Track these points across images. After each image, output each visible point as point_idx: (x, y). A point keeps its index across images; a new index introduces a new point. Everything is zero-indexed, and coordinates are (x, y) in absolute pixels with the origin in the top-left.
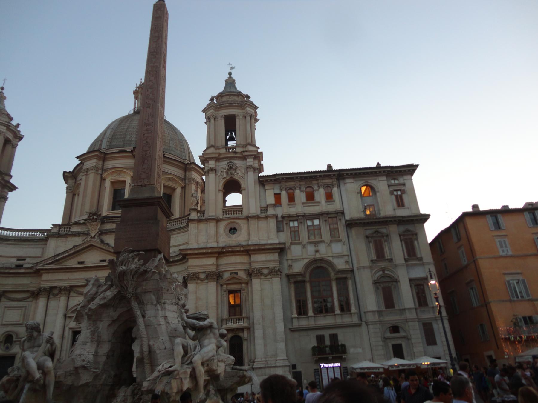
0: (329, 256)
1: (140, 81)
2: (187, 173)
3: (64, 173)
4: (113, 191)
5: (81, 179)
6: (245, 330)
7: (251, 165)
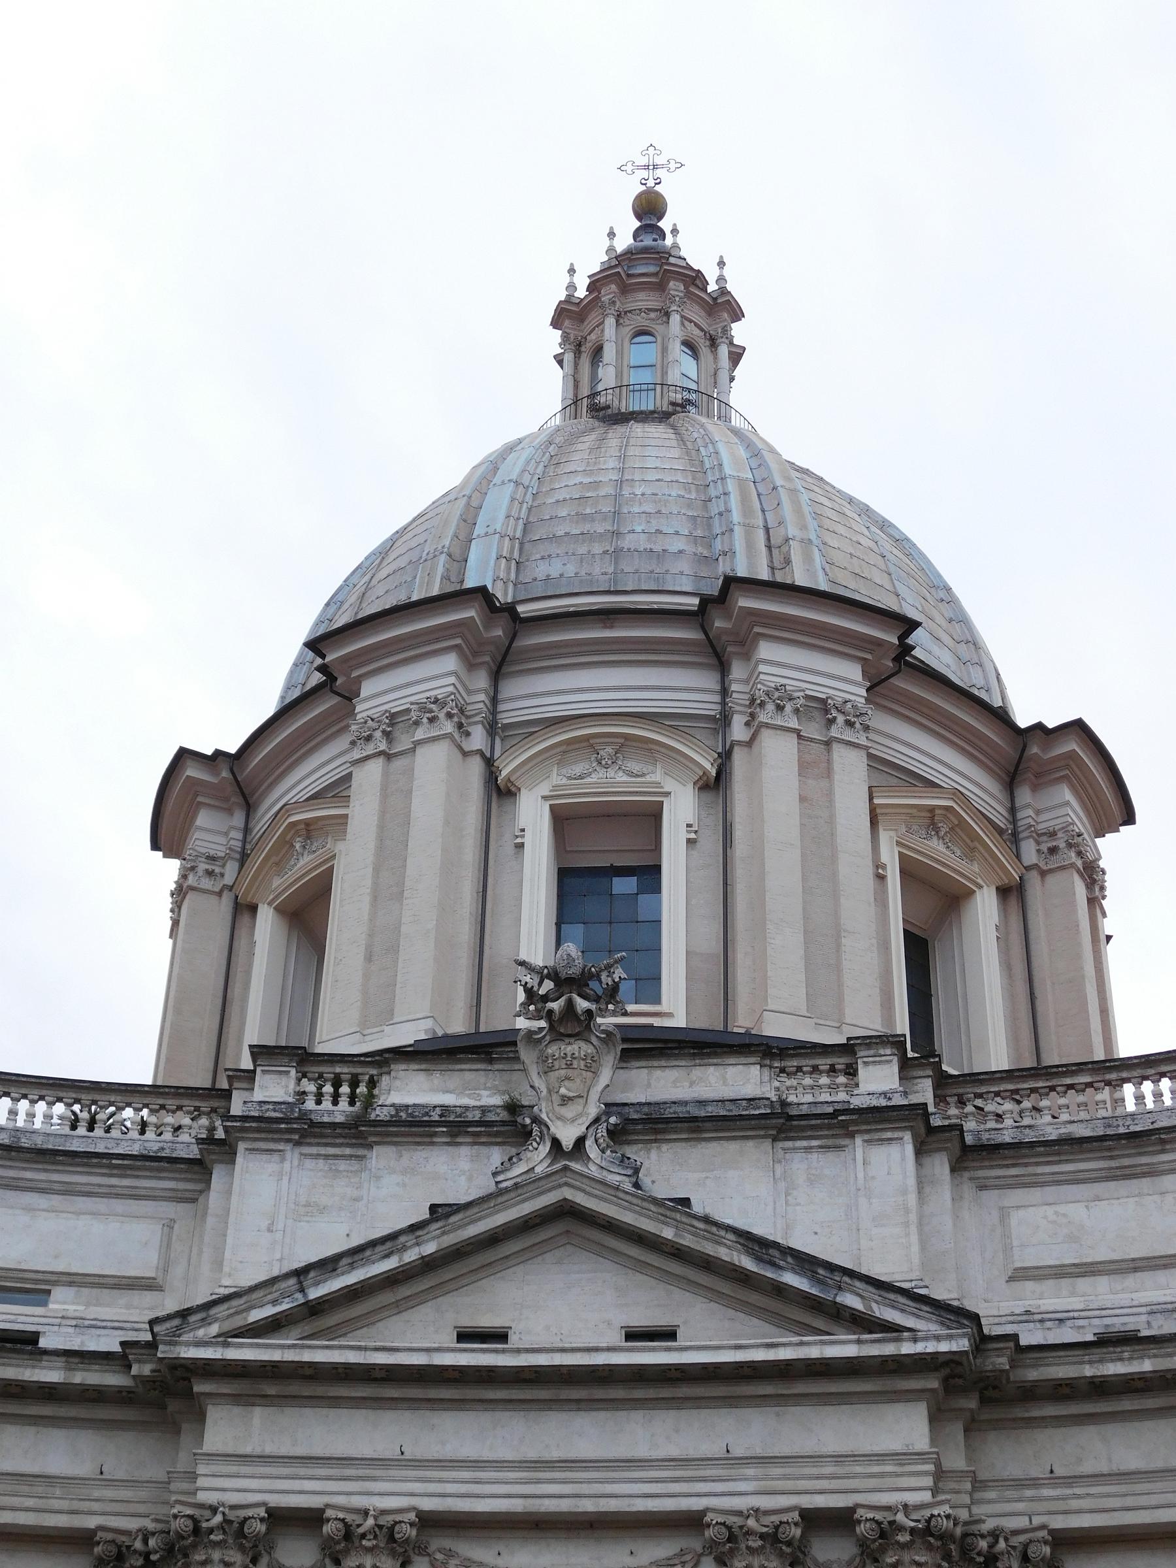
1: (606, 243)
2: (1024, 795)
3: (183, 755)
4: (556, 870)
5: (338, 790)
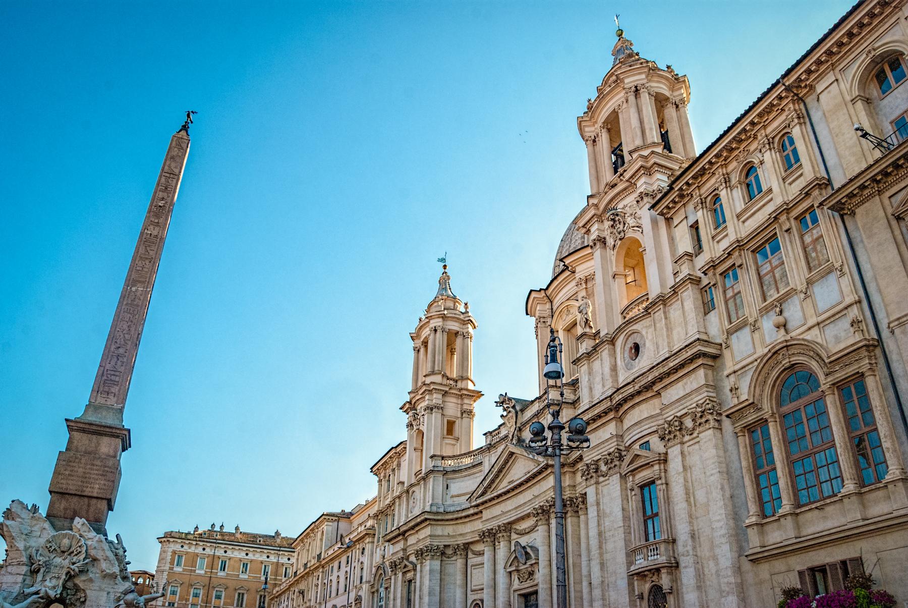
0: (809, 329)
6: (663, 571)
7: (641, 193)
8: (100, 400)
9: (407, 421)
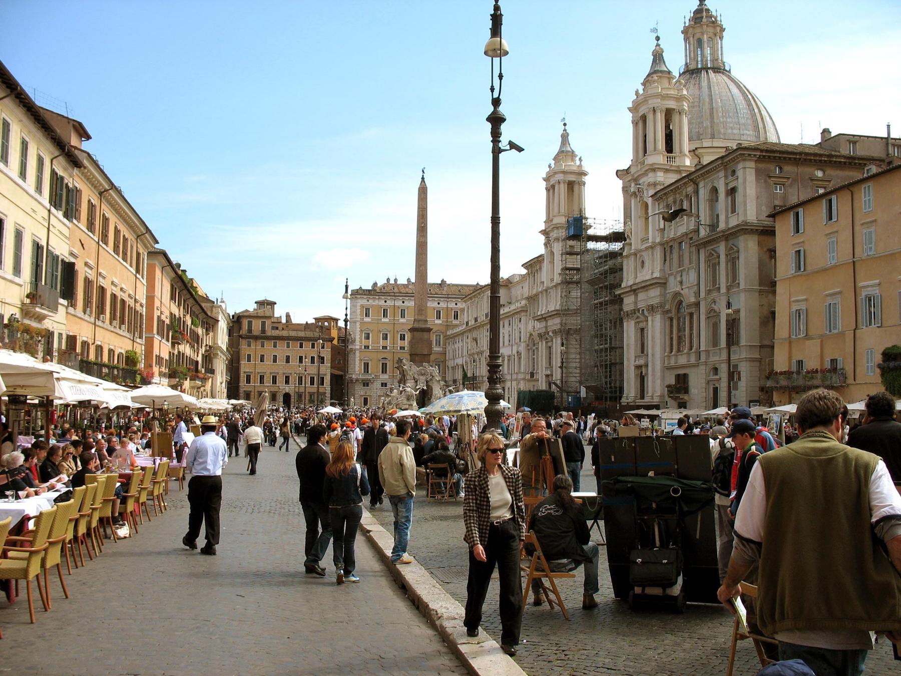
8: (420, 318)
9: (543, 242)
